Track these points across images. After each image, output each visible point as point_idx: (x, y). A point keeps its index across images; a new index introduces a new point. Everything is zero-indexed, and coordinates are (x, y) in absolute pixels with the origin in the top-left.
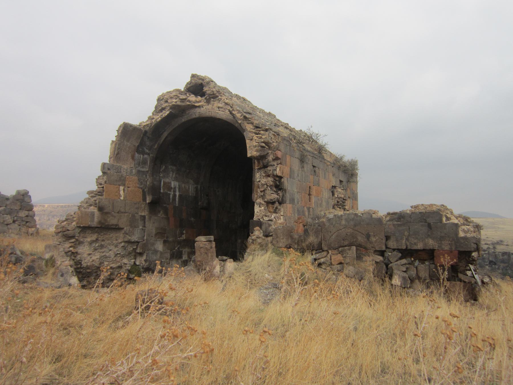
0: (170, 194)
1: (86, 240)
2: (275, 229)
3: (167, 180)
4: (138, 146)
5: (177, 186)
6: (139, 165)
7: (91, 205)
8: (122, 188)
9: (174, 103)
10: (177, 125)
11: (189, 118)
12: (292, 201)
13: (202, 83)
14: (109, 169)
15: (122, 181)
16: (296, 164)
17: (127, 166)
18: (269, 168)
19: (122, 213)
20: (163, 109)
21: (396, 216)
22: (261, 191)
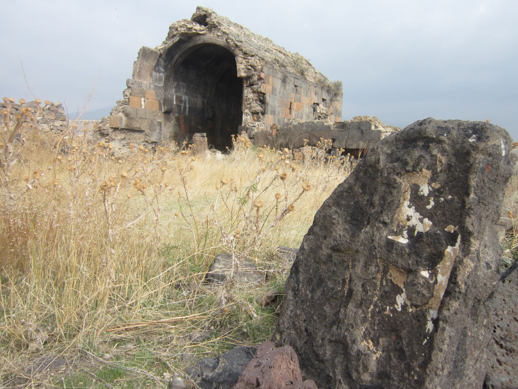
1: (117, 138)
2: (257, 133)
4: (155, 66)
5: (187, 100)
7: (120, 112)
9: (182, 31)
10: (185, 49)
11: (195, 44)
12: (273, 113)
13: (205, 15)
14: (132, 84)
15: (143, 94)
16: (278, 83)
17: (147, 82)
18: (254, 86)
20: (174, 36)
21: (341, 125)
22: (248, 104)
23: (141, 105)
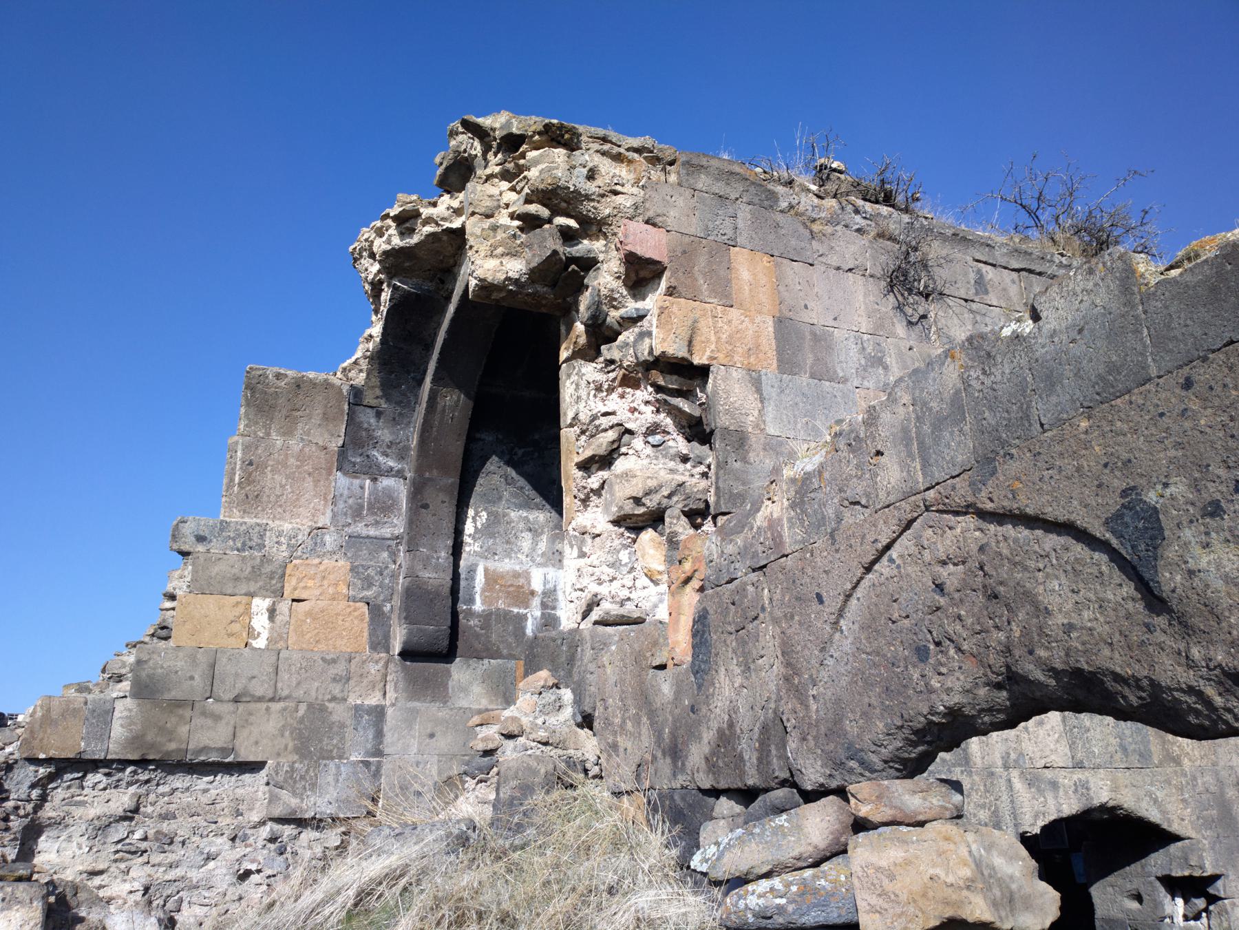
0: (522, 619)
3: (506, 565)
6: (357, 513)
8: (260, 605)
14: (201, 539)
15: (271, 580)
19: (260, 699)
23: (251, 633)
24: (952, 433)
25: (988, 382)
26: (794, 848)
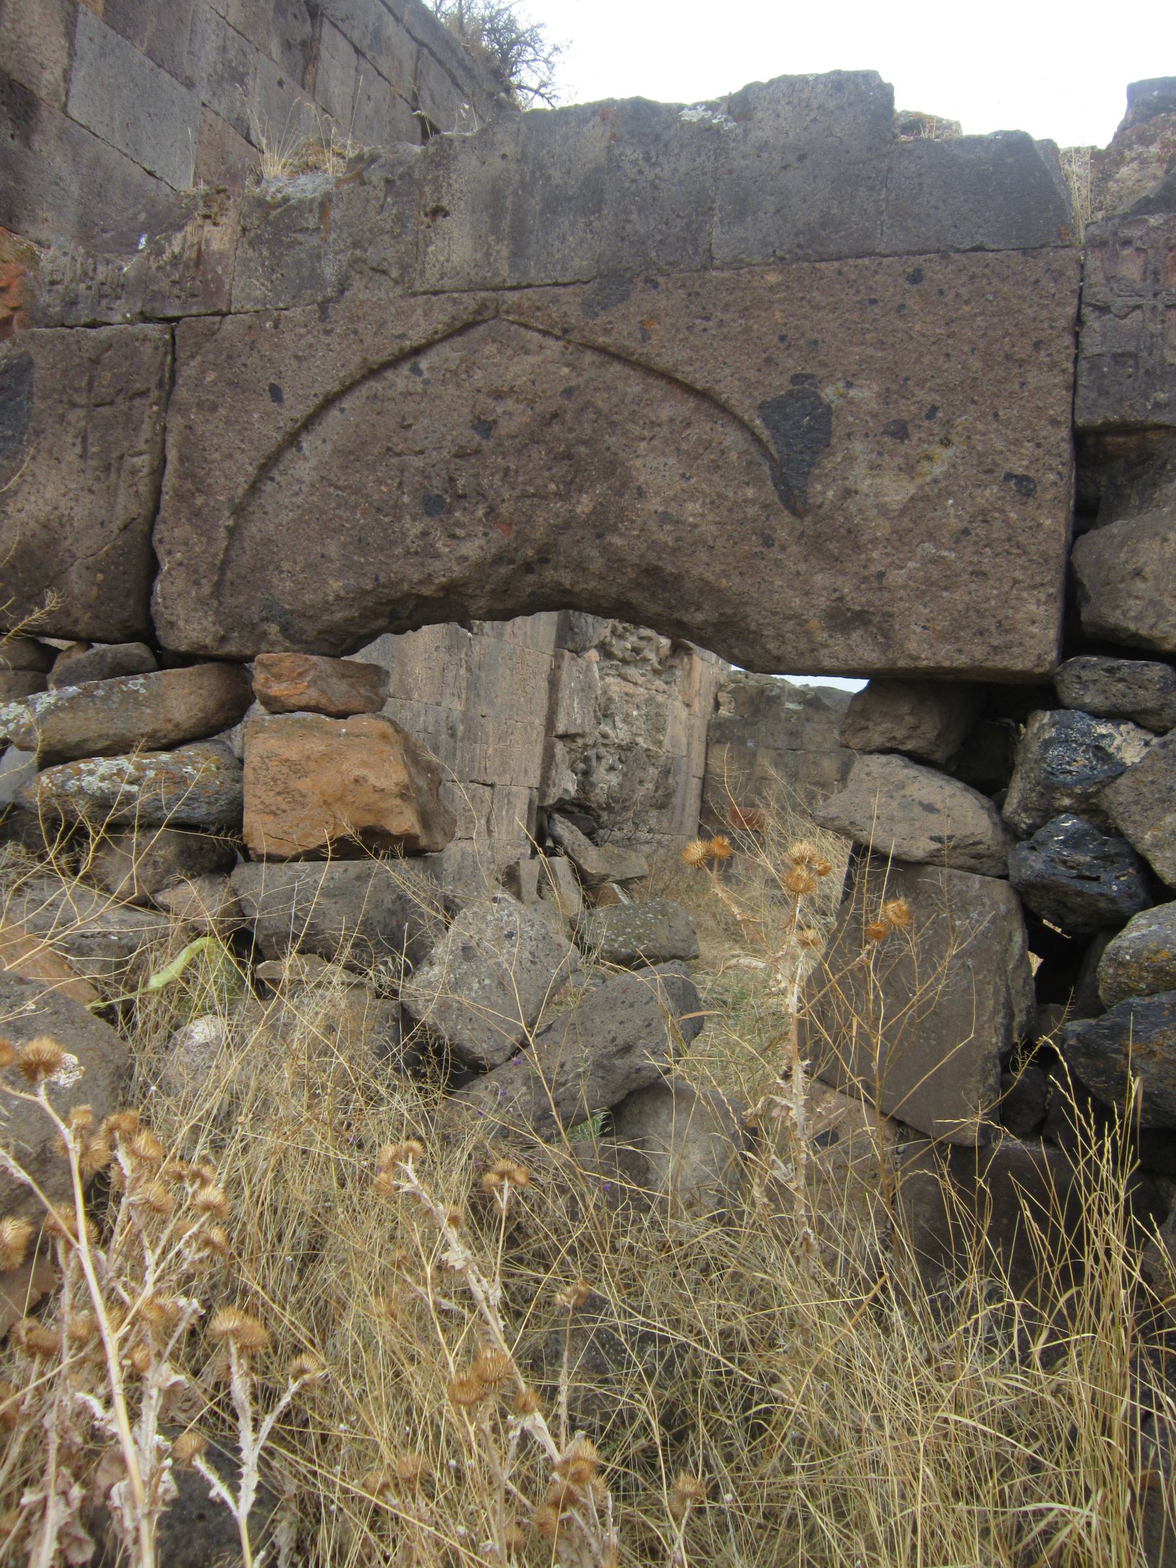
24: (573, 224)
25: (649, 173)
26: (146, 721)
